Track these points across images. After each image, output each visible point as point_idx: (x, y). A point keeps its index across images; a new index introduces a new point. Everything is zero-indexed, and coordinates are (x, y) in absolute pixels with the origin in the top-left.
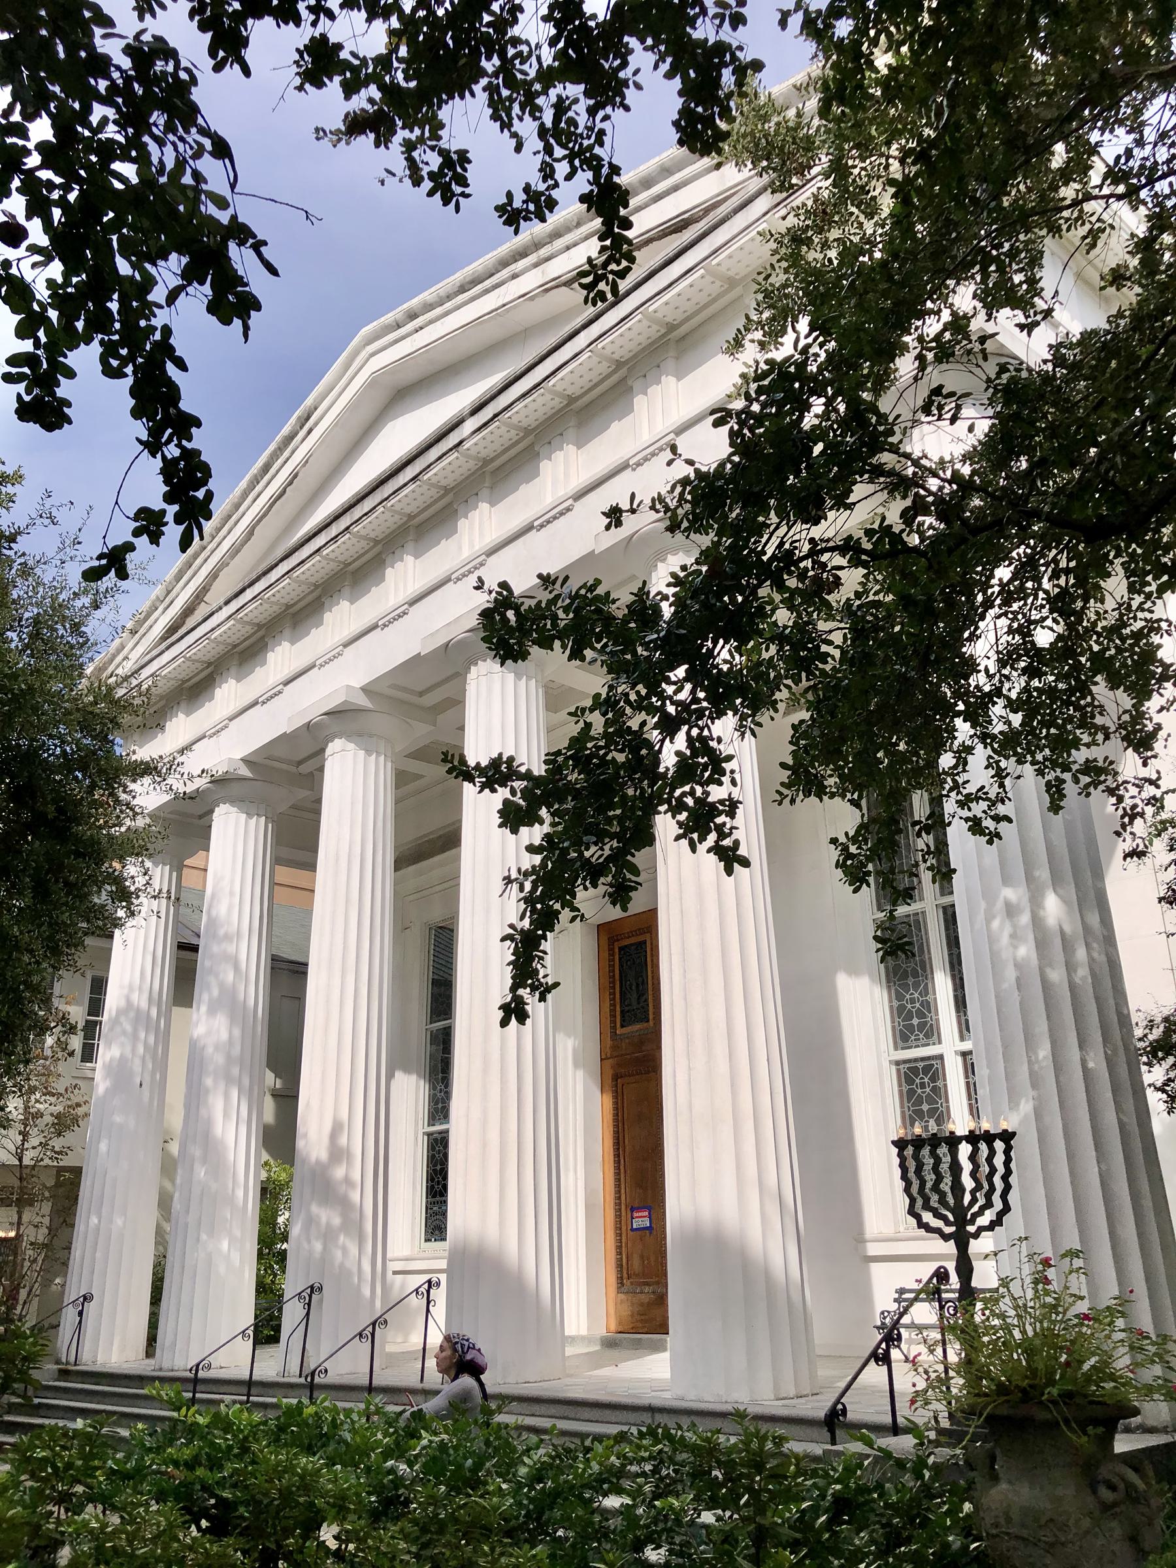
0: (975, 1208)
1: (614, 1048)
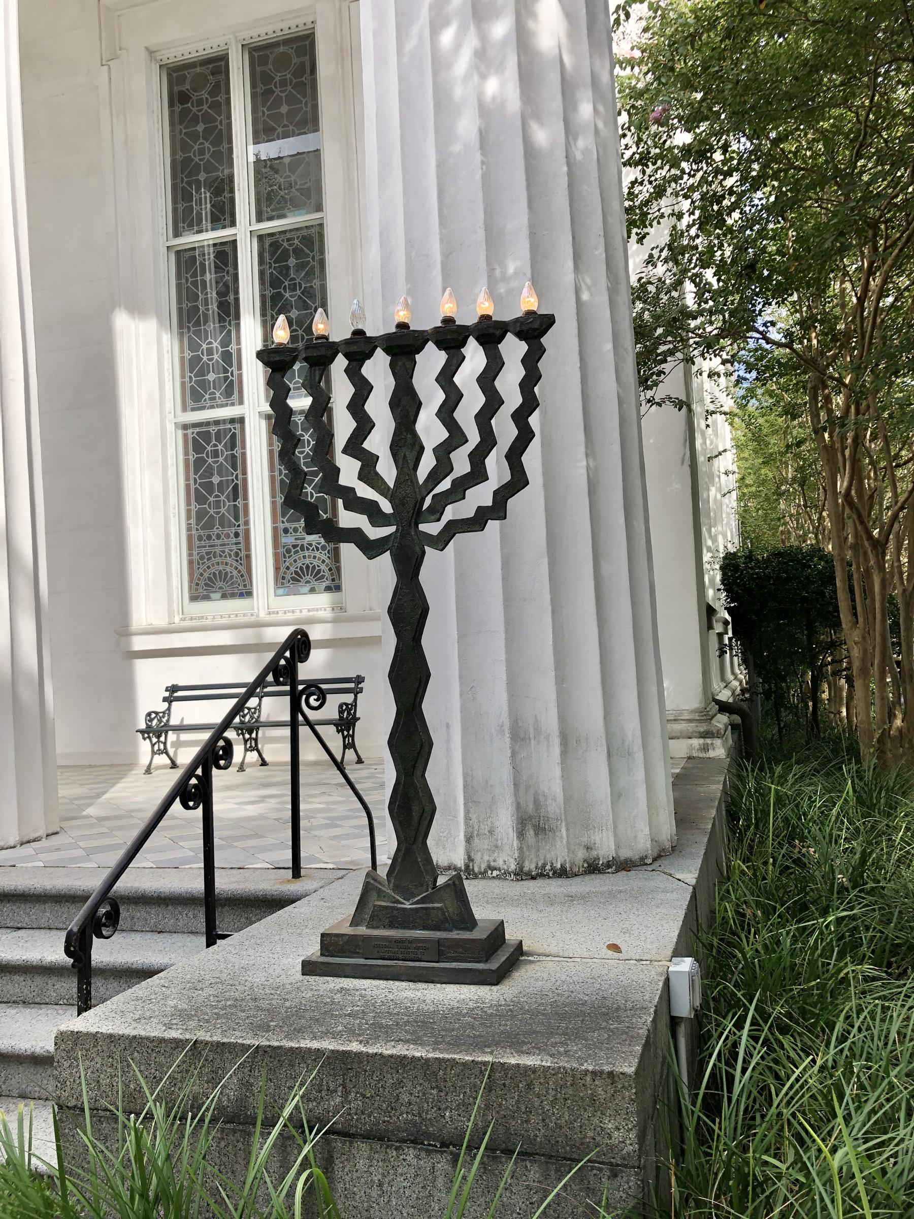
0: (445, 485)
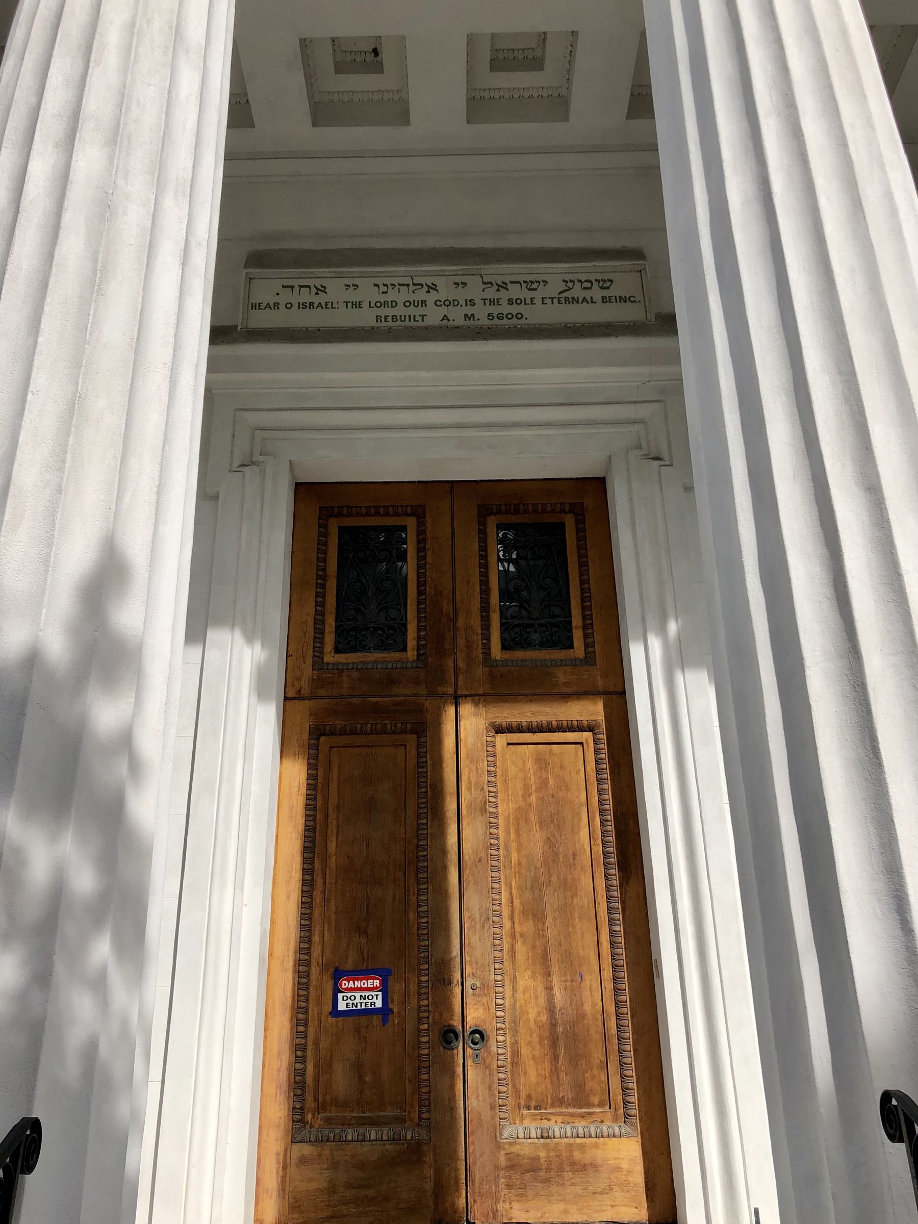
1: (318, 683)
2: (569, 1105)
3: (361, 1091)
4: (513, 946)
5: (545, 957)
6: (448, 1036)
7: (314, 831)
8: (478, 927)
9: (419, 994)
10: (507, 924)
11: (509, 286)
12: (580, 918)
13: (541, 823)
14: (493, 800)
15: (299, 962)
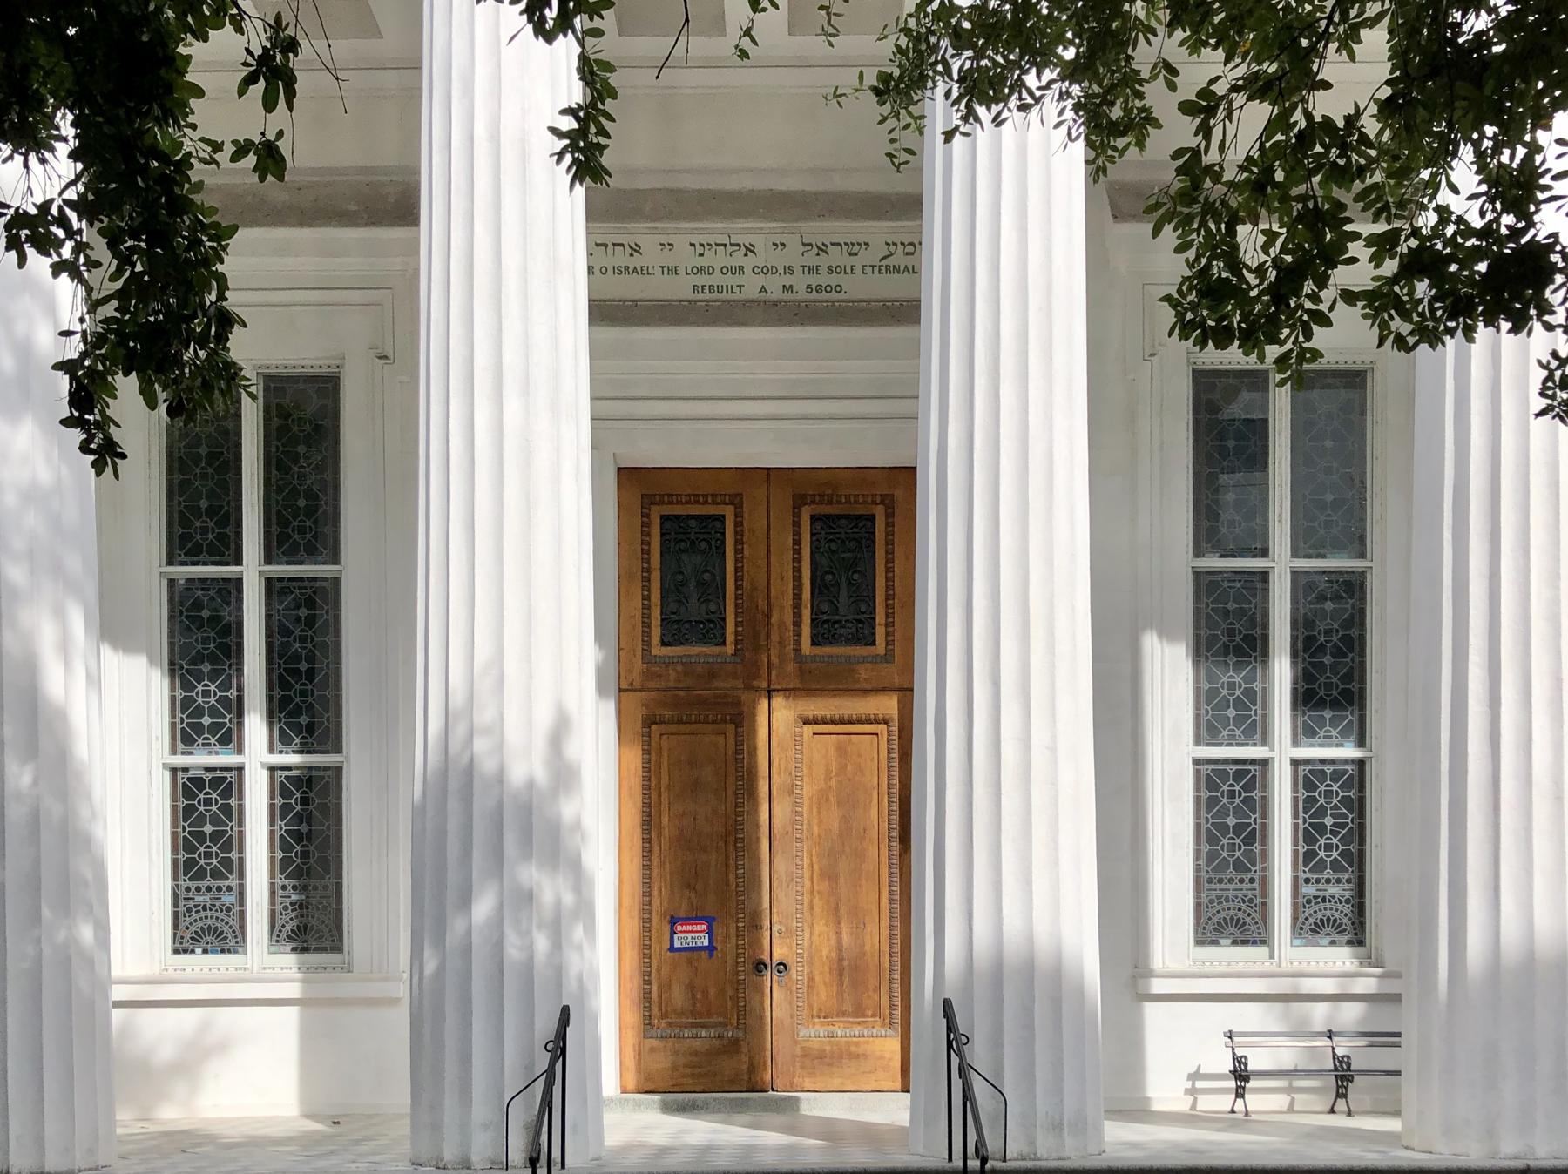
1: (648, 675)
2: (849, 1016)
3: (694, 1005)
4: (812, 901)
5: (837, 909)
6: (760, 966)
7: (650, 807)
8: (785, 885)
9: (738, 936)
10: (808, 884)
11: (831, 249)
12: (867, 881)
13: (840, 804)
14: (799, 783)
15: (643, 911)
